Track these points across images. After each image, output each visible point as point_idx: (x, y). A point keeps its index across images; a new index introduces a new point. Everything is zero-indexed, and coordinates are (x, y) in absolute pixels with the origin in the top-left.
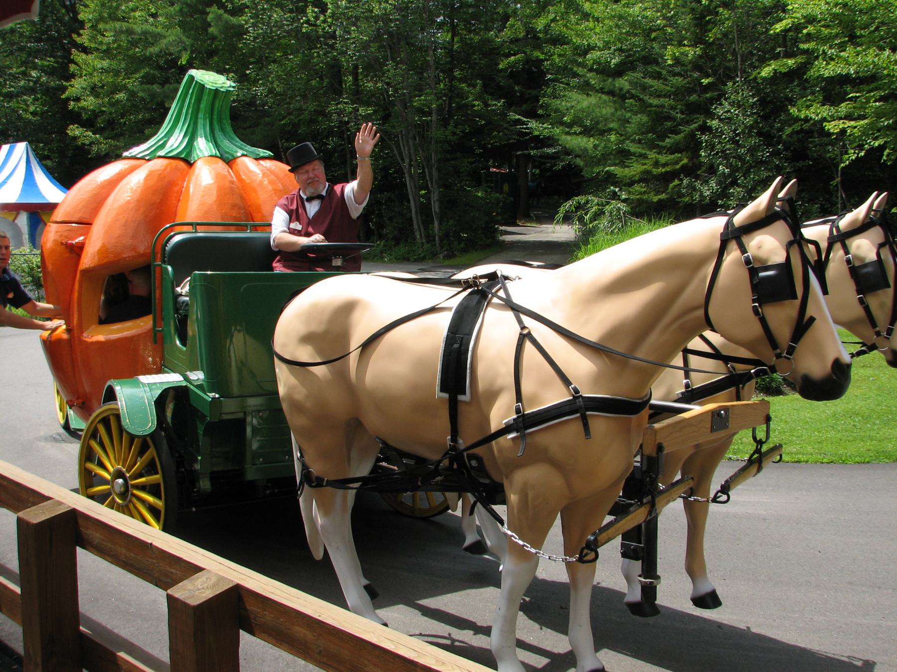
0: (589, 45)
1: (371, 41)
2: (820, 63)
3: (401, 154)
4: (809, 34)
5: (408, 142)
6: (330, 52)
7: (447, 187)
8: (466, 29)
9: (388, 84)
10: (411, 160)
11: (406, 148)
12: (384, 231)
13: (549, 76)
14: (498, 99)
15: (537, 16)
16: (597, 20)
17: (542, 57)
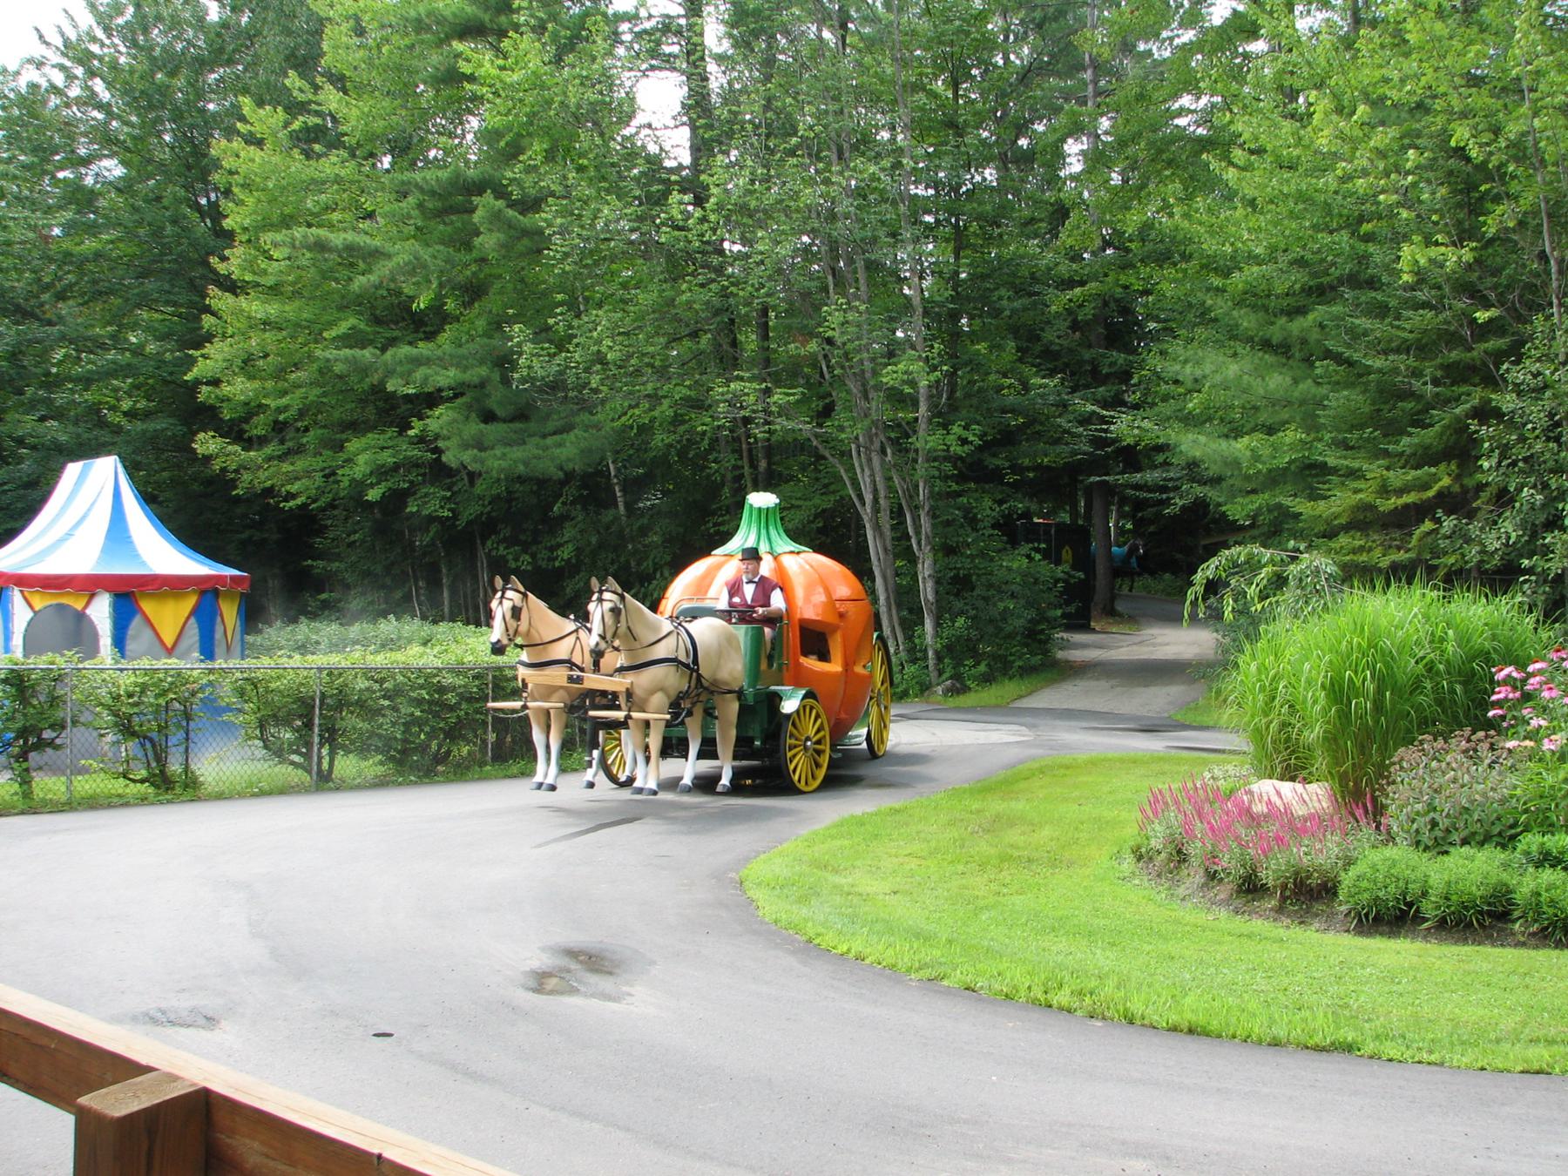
5: (870, 460)
6: (713, 281)
11: (867, 472)
14: (1051, 375)
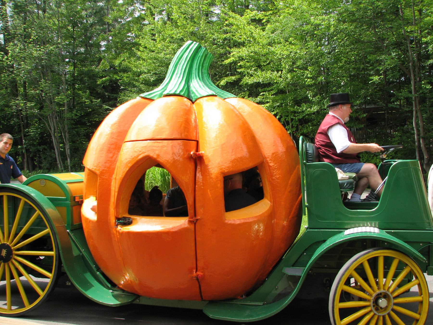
0: (140, 71)
1: (32, 70)
2: (246, 77)
3: (49, 126)
4: (240, 66)
5: (53, 120)
6: (11, 75)
7: (74, 142)
8: (81, 65)
9: (42, 91)
10: (55, 130)
11: (52, 123)
12: (42, 165)
13: (122, 87)
14: (98, 99)
15: (115, 59)
16: (144, 60)
17: (118, 78)
